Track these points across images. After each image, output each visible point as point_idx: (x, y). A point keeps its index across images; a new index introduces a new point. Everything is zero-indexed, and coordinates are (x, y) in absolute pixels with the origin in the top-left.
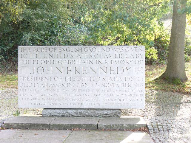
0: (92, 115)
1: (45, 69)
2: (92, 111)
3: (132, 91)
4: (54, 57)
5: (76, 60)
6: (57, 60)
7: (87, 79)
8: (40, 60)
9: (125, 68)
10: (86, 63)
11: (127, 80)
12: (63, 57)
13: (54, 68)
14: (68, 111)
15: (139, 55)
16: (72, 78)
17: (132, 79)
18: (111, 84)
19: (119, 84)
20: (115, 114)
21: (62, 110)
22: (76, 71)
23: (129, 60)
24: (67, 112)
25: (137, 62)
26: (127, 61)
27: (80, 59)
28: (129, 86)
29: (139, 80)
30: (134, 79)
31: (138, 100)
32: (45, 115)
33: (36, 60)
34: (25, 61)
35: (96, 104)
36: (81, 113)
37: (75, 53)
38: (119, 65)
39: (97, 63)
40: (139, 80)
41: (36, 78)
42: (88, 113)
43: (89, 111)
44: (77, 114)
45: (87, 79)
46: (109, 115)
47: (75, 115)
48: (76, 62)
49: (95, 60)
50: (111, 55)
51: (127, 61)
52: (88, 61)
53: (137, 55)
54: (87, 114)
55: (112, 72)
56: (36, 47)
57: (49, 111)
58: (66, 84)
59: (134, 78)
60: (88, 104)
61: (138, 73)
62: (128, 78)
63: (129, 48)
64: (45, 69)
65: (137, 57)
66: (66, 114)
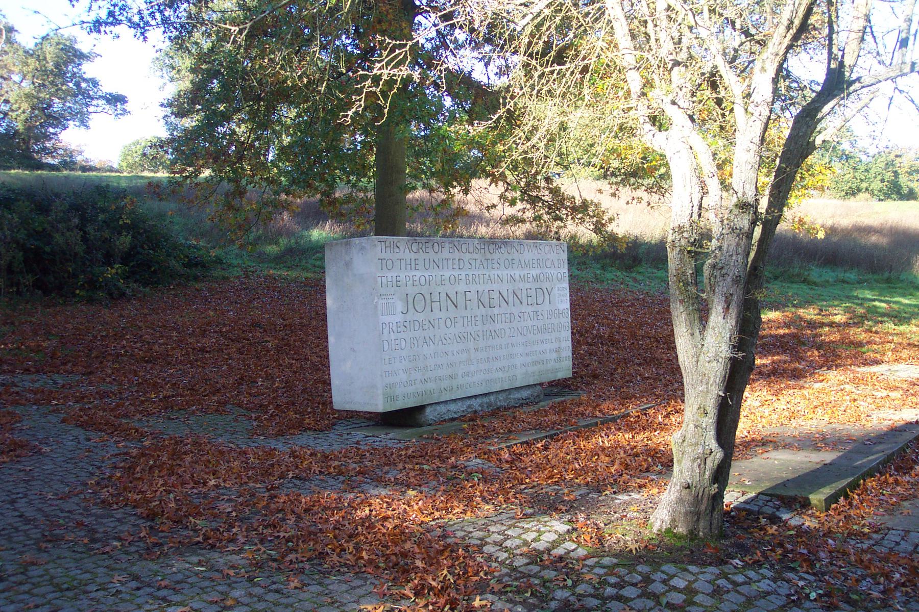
1: (428, 297)
2: (504, 395)
4: (441, 267)
6: (447, 274)
8: (418, 274)
12: (456, 266)
13: (443, 295)
14: (468, 402)
21: (460, 404)
24: (469, 407)
37: (475, 256)
41: (412, 322)
48: (477, 280)
49: (506, 272)
57: (438, 408)
58: (465, 335)
64: (428, 297)
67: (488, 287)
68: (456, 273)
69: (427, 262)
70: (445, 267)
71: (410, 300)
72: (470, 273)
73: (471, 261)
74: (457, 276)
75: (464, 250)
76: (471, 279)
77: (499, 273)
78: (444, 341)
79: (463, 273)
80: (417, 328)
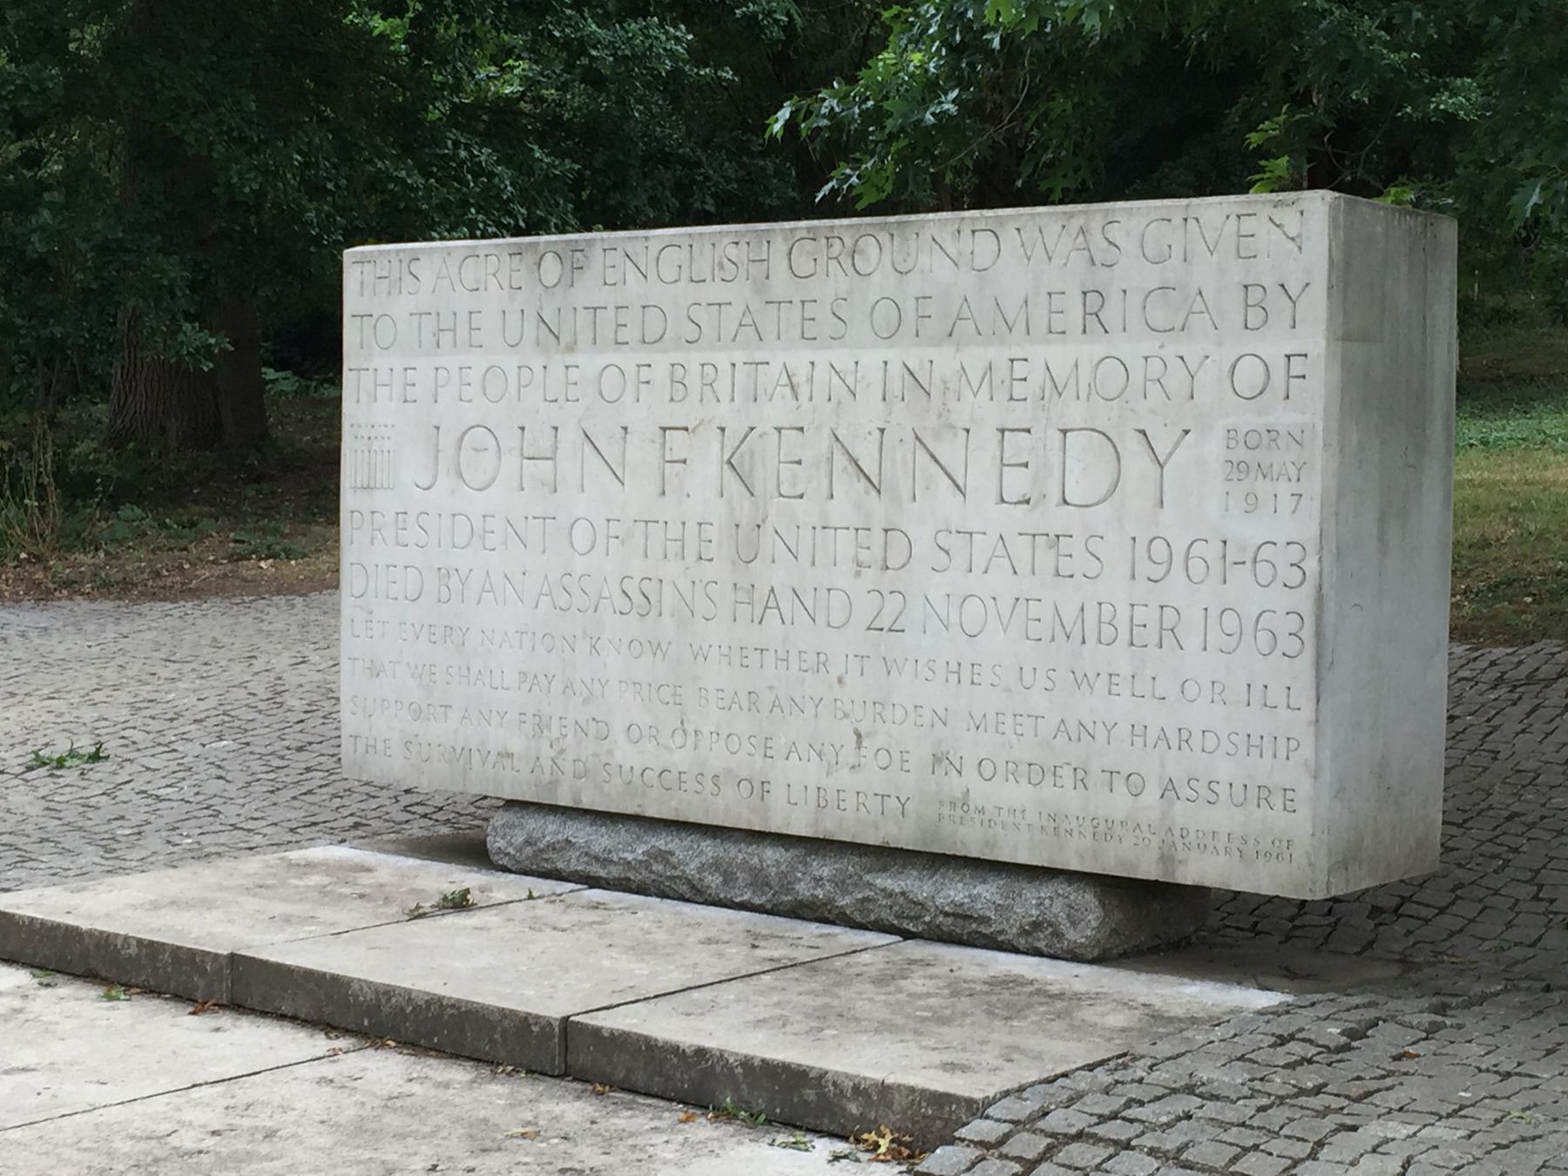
0: (843, 901)
2: (850, 865)
3: (1191, 689)
4: (566, 338)
5: (724, 366)
7: (805, 558)
8: (479, 362)
9: (1132, 447)
10: (804, 391)
11: (1144, 569)
14: (661, 842)
15: (1277, 302)
16: (692, 528)
17: (1197, 567)
18: (1005, 605)
19: (1070, 614)
20: (1036, 926)
21: (623, 834)
22: (725, 466)
23: (1170, 352)
24: (663, 856)
25: (1250, 373)
26: (1155, 366)
27: (759, 357)
28: (1168, 638)
29: (1264, 570)
30: (1216, 567)
31: (1253, 792)
32: (505, 861)
33: (451, 361)
34: (383, 376)
35: (874, 804)
36: (759, 879)
38: (1076, 413)
39: (895, 388)
40: (1264, 570)
42: (818, 880)
43: (824, 868)
44: (728, 879)
45: (805, 558)
46: (985, 920)
47: (713, 881)
48: (723, 387)
49: (872, 358)
50: (1012, 309)
51: (1155, 366)
52: (821, 373)
53: (1255, 295)
54: (804, 889)
55: (1016, 483)
56: (398, 252)
59: (1212, 551)
60: (812, 792)
61: (1252, 505)
62: (1159, 550)
63: (1178, 220)
64: (510, 439)
65: (1255, 317)
66: (648, 866)
67: (776, 411)
68: (628, 360)
69: (513, 318)
70: (585, 337)
71: (447, 441)
72: (693, 358)
73: (699, 314)
74: (631, 371)
75: (669, 273)
76: (693, 380)
77: (841, 357)
78: (562, 599)
79: (661, 362)
80: (461, 539)
